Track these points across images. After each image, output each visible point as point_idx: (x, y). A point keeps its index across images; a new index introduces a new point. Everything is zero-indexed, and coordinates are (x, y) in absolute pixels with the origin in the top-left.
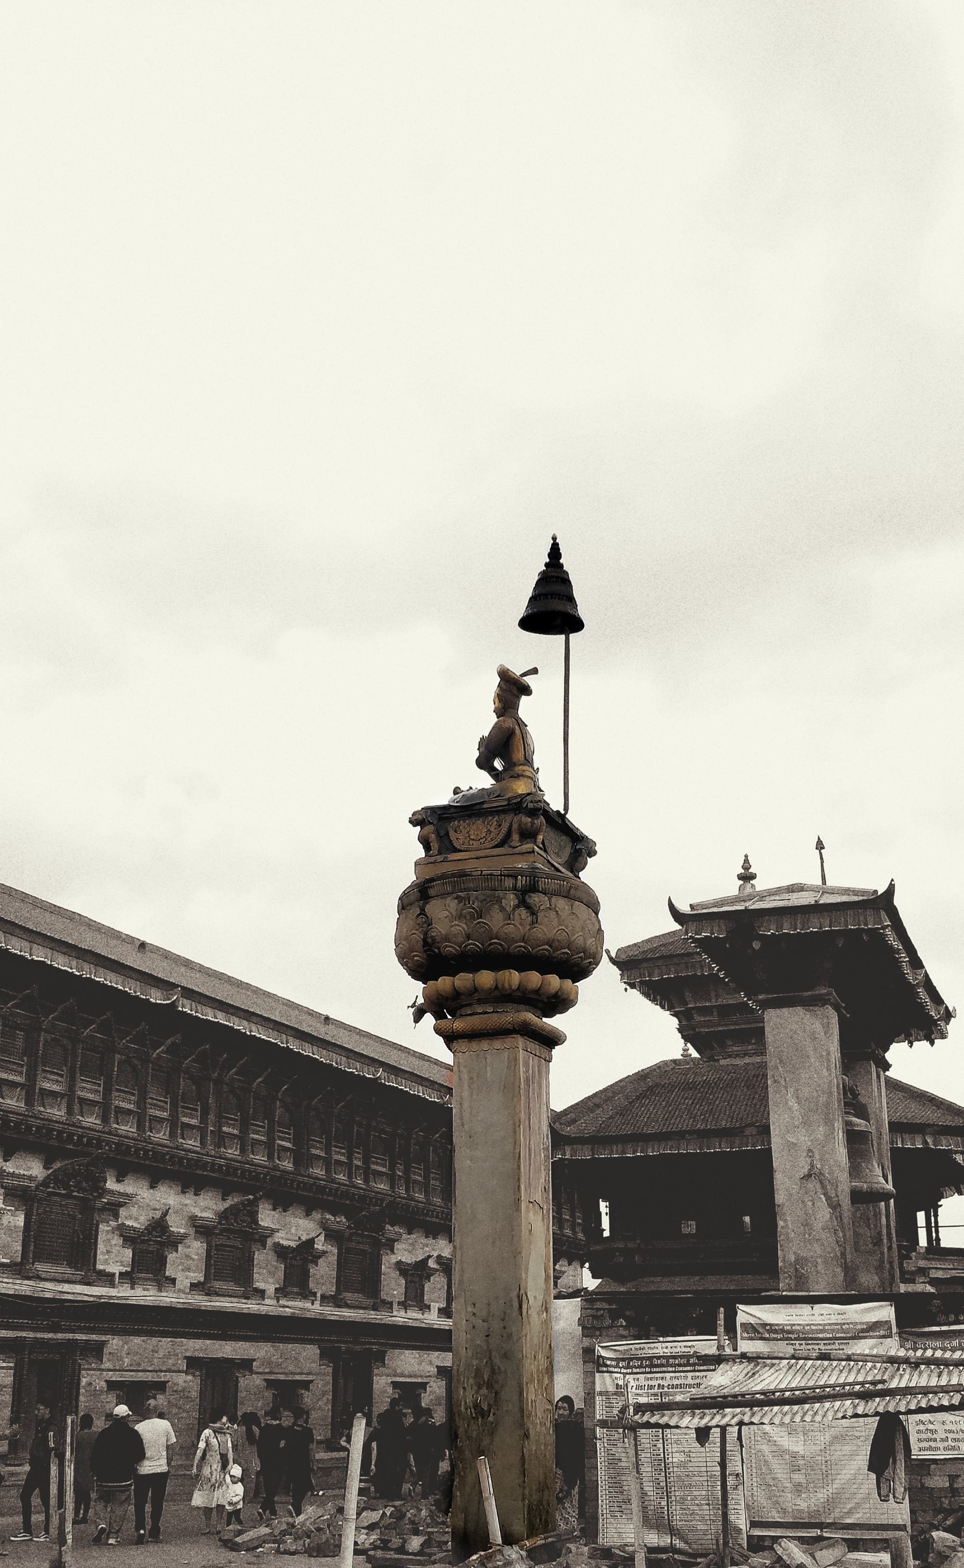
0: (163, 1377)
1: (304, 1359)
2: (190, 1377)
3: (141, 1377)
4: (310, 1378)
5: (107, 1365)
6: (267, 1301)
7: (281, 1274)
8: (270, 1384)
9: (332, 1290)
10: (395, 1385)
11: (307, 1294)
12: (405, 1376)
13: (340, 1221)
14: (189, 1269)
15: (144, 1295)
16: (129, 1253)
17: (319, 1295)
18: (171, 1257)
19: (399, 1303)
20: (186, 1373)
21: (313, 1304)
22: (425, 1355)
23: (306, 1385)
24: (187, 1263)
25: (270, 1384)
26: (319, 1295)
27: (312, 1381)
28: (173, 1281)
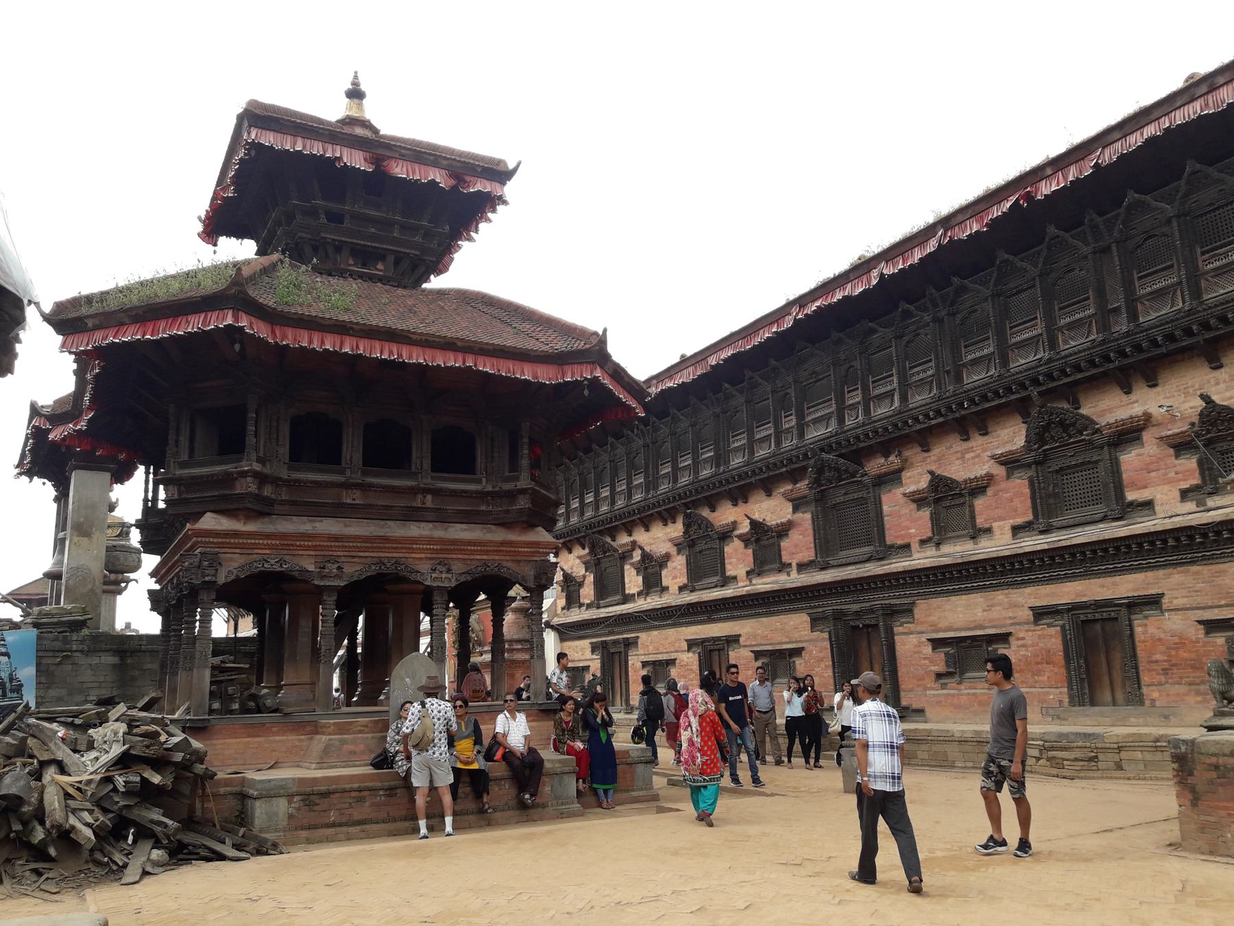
0: (673, 656)
1: (793, 628)
2: (691, 655)
3: (660, 657)
4: (800, 645)
5: (641, 652)
6: (741, 584)
7: (751, 559)
8: (758, 655)
9: (808, 554)
10: (937, 643)
11: (784, 567)
12: (956, 630)
13: (803, 485)
14: (675, 577)
15: (653, 602)
16: (640, 578)
17: (794, 565)
18: (664, 573)
19: (923, 542)
20: (689, 650)
21: (789, 575)
22: (1000, 596)
23: (798, 652)
24: (675, 574)
25: (758, 655)
26: (794, 565)
27: (803, 648)
28: (667, 588)
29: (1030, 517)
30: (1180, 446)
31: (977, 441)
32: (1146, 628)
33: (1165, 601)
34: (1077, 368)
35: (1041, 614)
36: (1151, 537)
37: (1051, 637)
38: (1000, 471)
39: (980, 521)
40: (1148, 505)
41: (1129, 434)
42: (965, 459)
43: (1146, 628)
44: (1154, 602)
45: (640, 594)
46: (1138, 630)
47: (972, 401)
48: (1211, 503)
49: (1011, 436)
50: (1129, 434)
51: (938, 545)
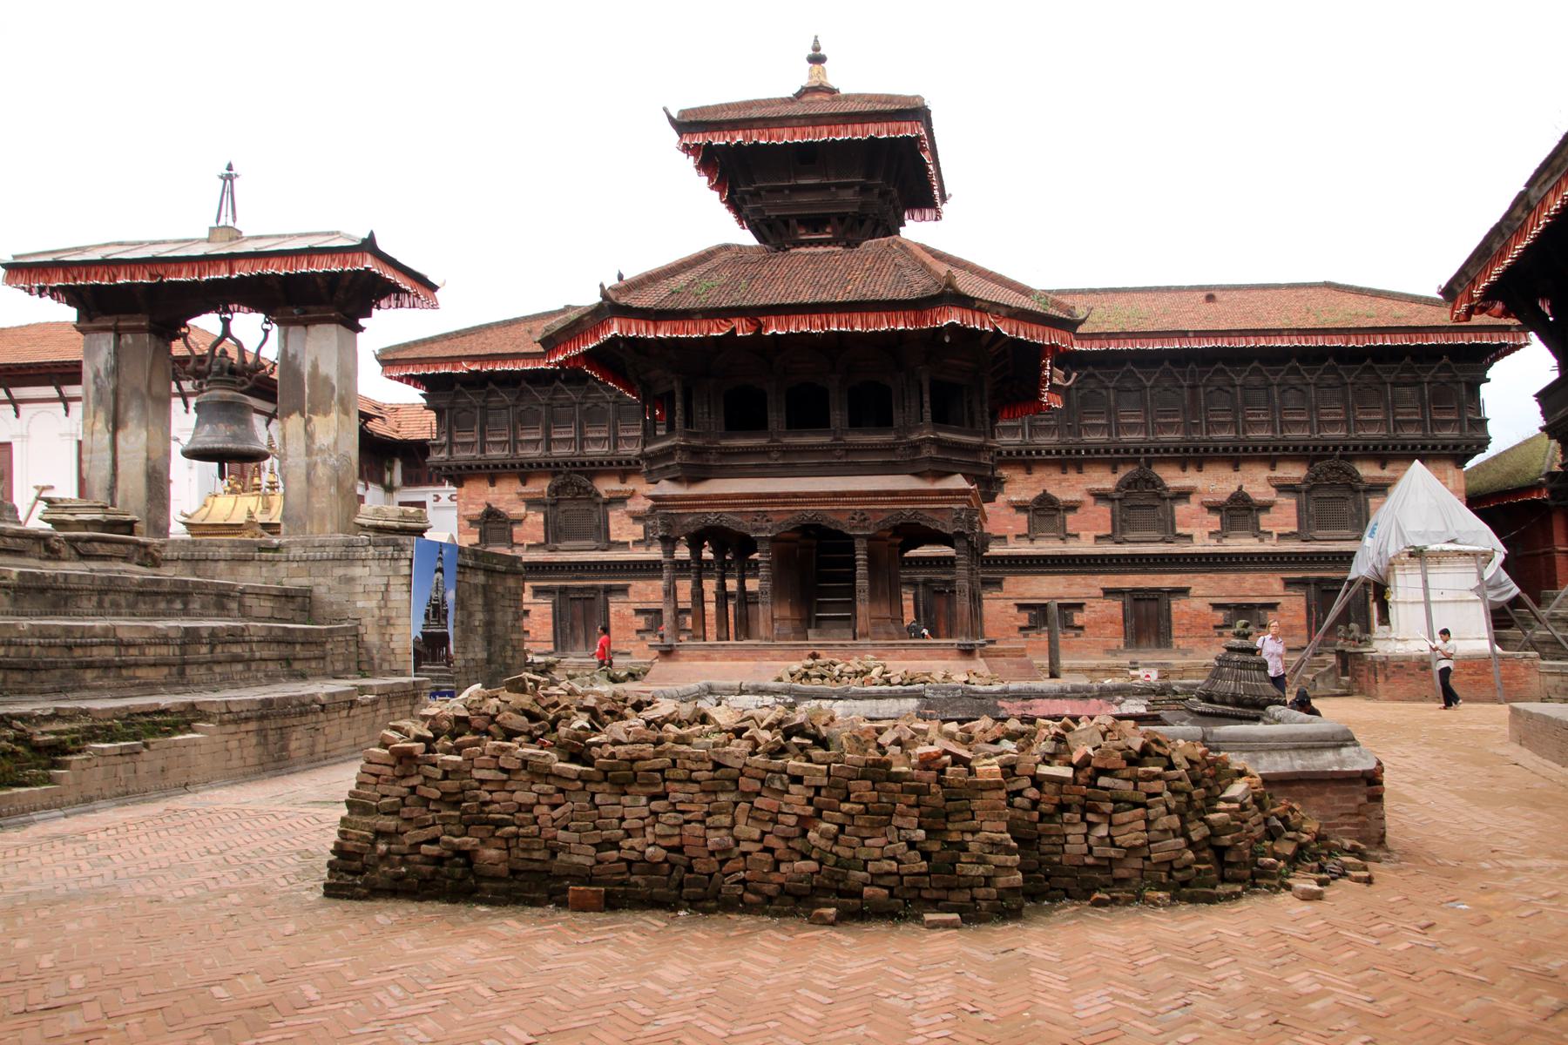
29: (1109, 532)
30: (1213, 508)
31: (1072, 476)
32: (1178, 606)
33: (1192, 592)
34: (1167, 450)
35: (1109, 593)
36: (1193, 556)
37: (1115, 607)
38: (1091, 500)
39: (1070, 529)
40: (1190, 537)
41: (1184, 495)
42: (1068, 487)
43: (1178, 606)
44: (1184, 592)
45: (635, 542)
46: (1174, 606)
47: (1088, 452)
48: (1225, 541)
49: (1105, 480)
50: (1184, 495)
51: (1032, 540)
